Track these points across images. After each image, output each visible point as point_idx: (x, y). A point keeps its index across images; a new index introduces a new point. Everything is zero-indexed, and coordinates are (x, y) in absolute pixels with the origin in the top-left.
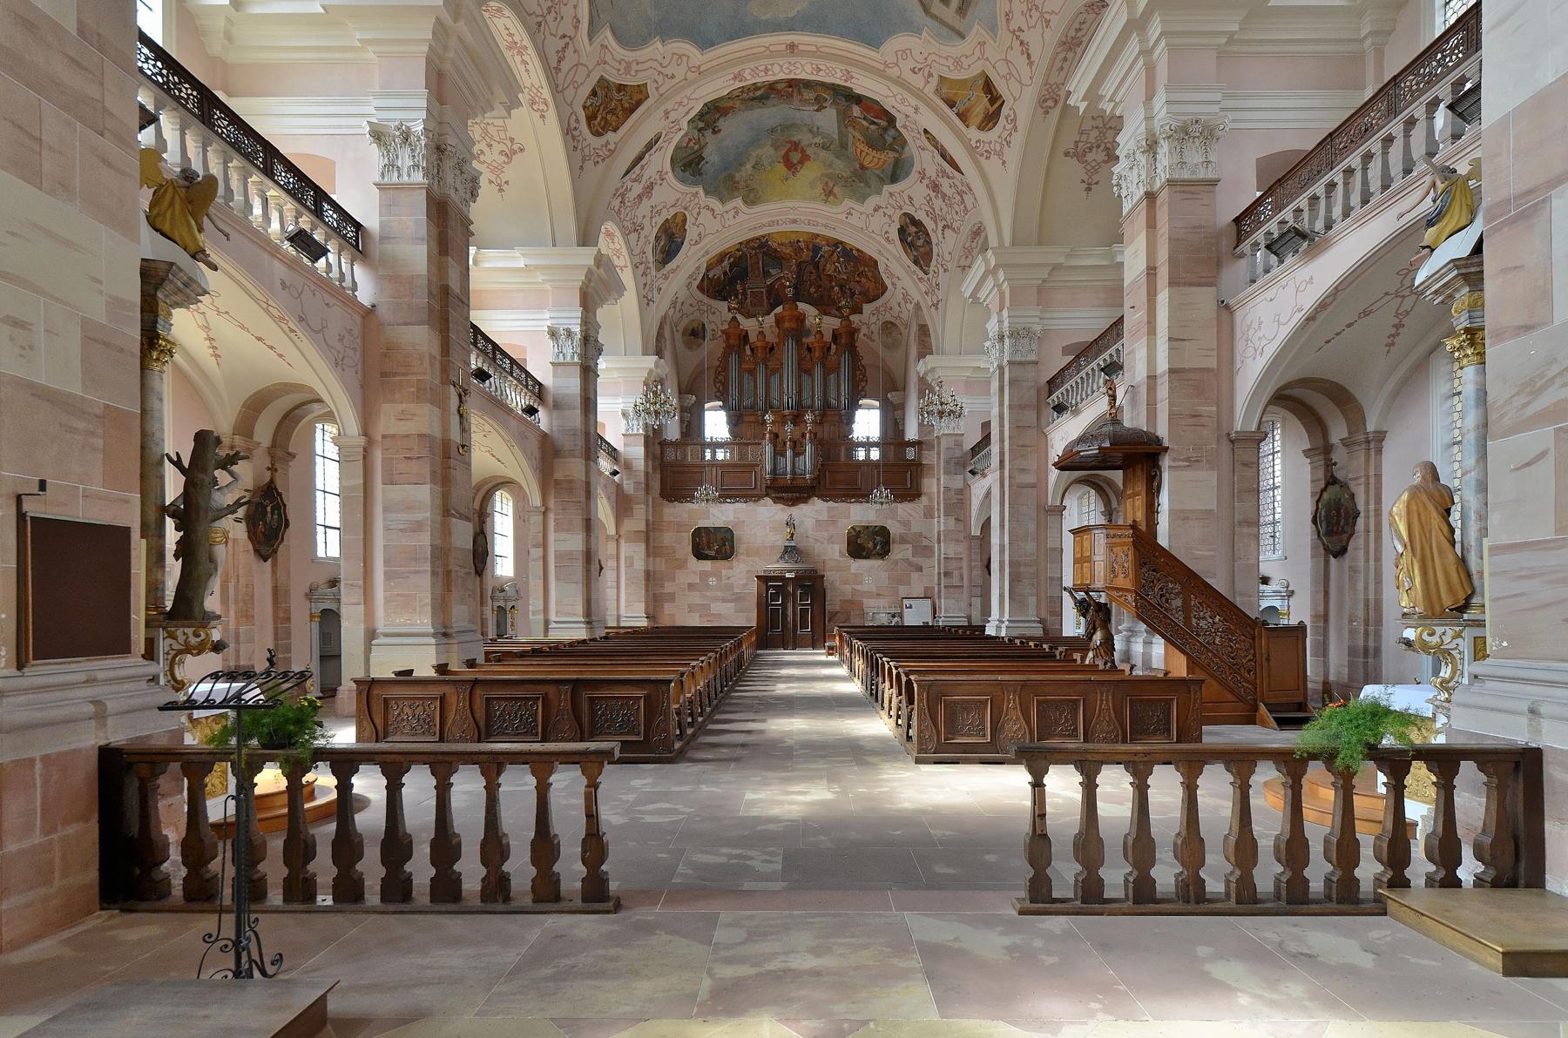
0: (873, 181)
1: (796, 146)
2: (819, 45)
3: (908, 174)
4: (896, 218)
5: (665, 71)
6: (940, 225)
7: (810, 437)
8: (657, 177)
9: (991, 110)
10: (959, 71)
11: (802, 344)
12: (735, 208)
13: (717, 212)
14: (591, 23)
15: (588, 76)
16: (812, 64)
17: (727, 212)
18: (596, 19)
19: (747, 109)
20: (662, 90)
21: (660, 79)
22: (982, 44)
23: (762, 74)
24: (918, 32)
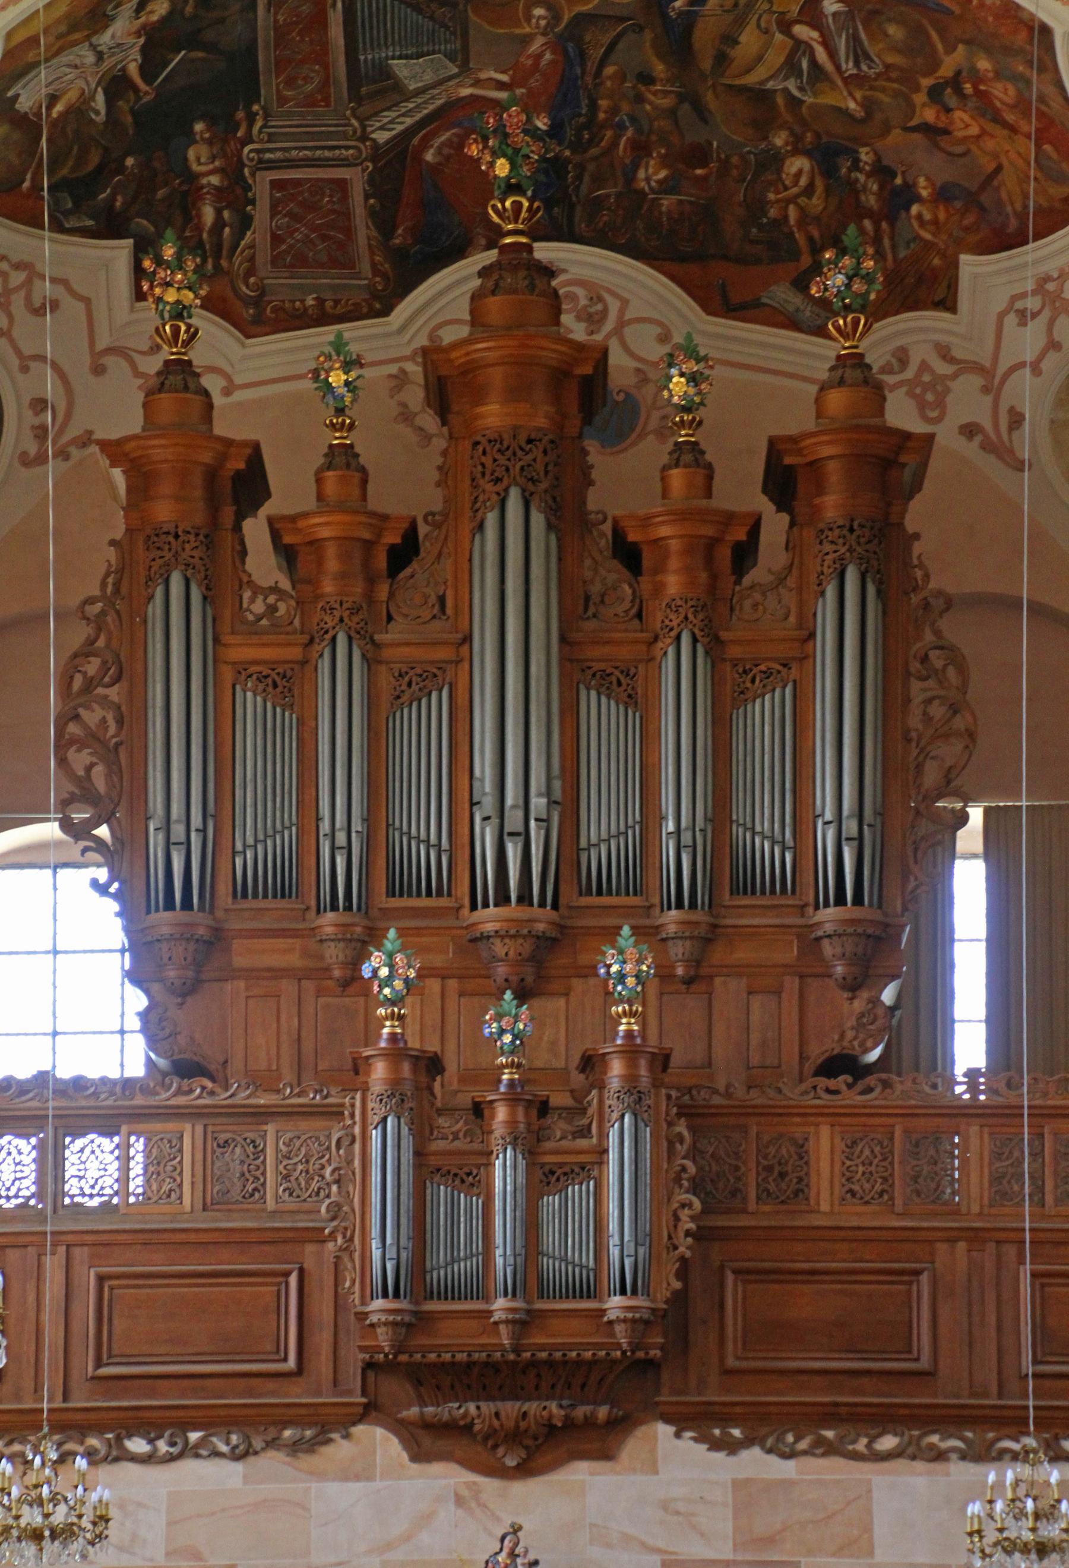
7: (631, 1079)
11: (584, 523)
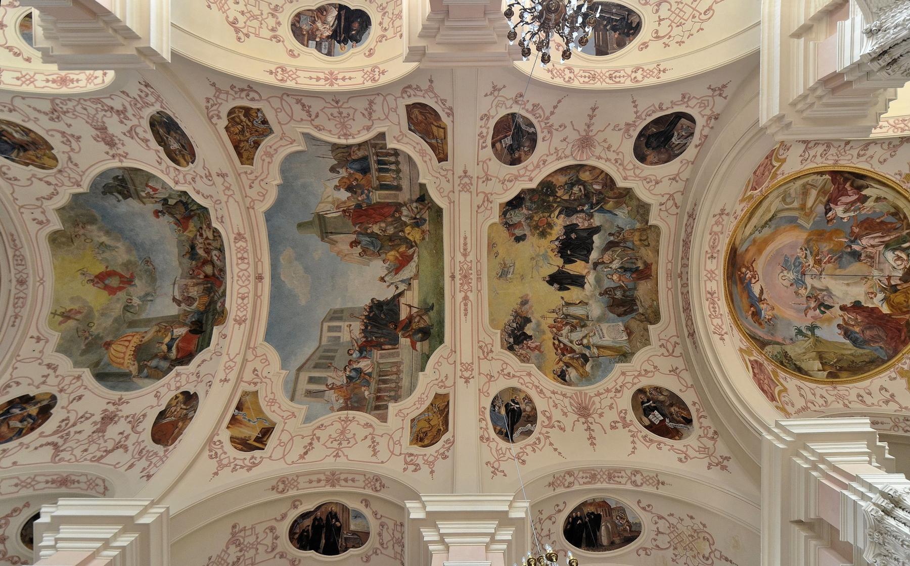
0: (93, 357)
1: (129, 281)
2: (262, 297)
3: (113, 388)
4: (44, 389)
5: (257, 182)
6: (54, 439)
8: (120, 152)
9: (251, 442)
10: (267, 405)
12: (48, 221)
13: (46, 203)
14: (314, 139)
15: (279, 123)
16: (248, 293)
17: (43, 212)
18: (314, 142)
19: (180, 243)
20: (243, 176)
21: (252, 177)
22: (294, 415)
23: (239, 255)
24: (283, 367)
